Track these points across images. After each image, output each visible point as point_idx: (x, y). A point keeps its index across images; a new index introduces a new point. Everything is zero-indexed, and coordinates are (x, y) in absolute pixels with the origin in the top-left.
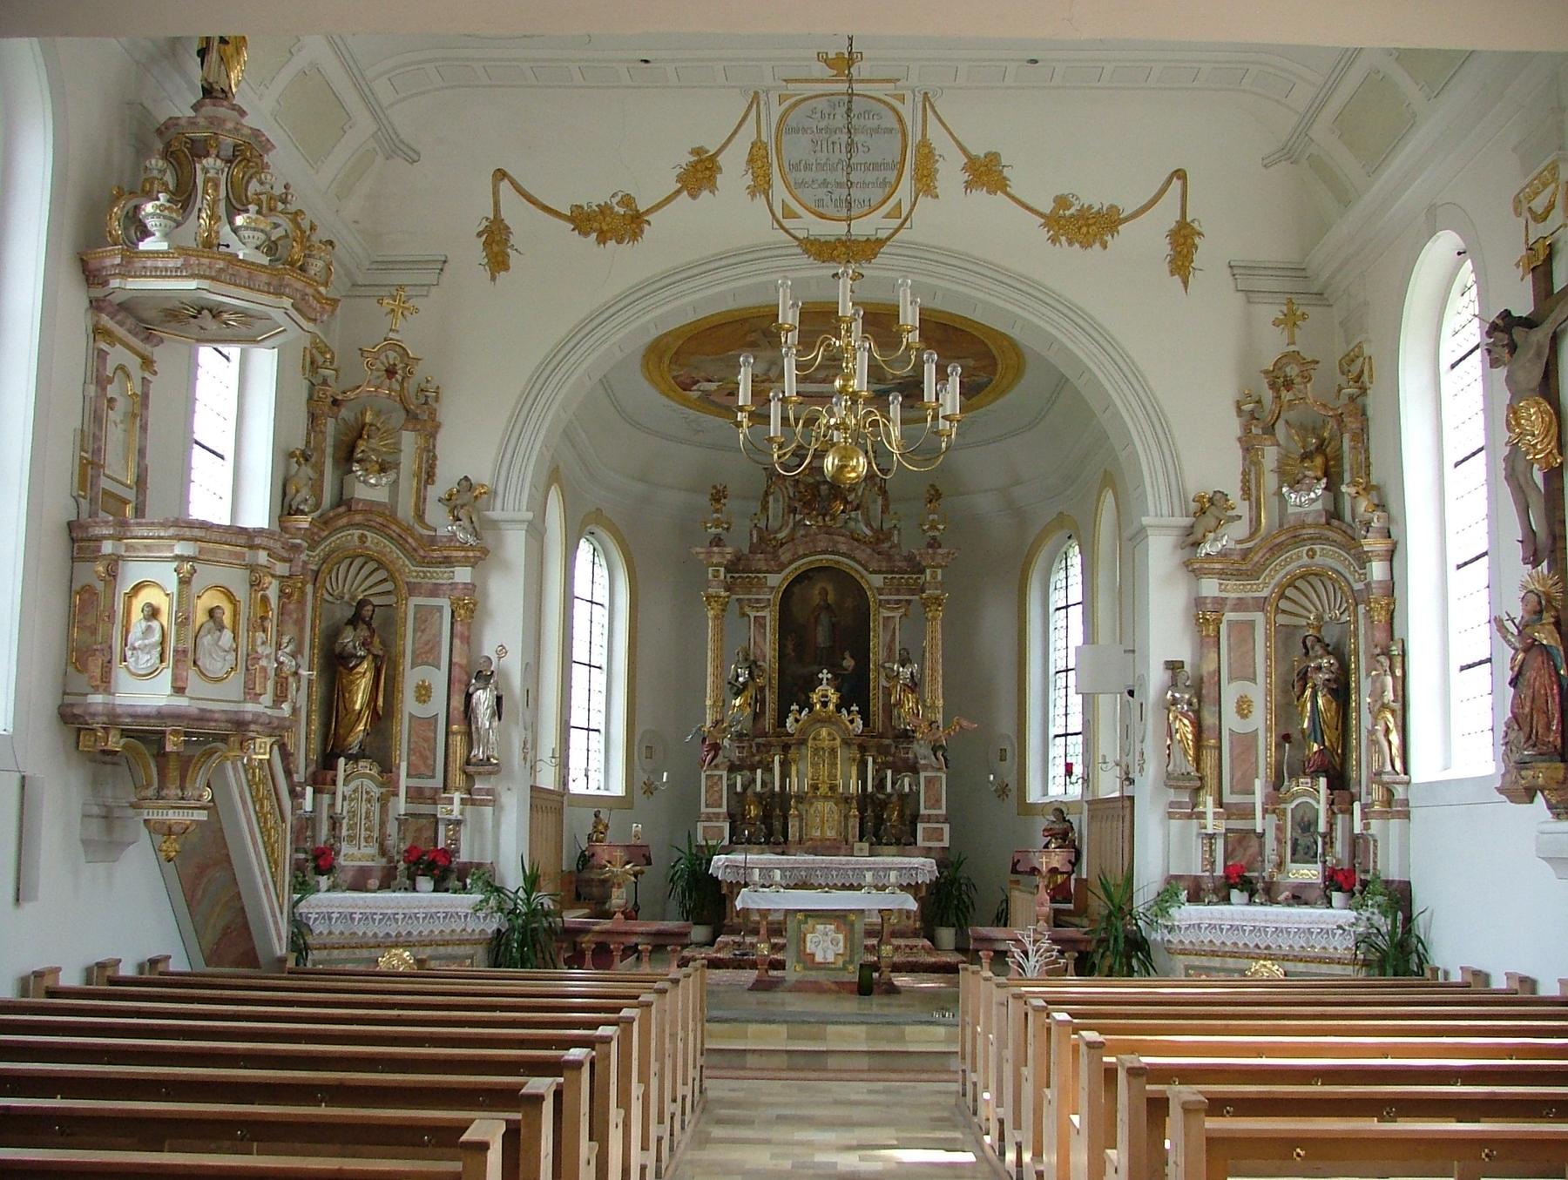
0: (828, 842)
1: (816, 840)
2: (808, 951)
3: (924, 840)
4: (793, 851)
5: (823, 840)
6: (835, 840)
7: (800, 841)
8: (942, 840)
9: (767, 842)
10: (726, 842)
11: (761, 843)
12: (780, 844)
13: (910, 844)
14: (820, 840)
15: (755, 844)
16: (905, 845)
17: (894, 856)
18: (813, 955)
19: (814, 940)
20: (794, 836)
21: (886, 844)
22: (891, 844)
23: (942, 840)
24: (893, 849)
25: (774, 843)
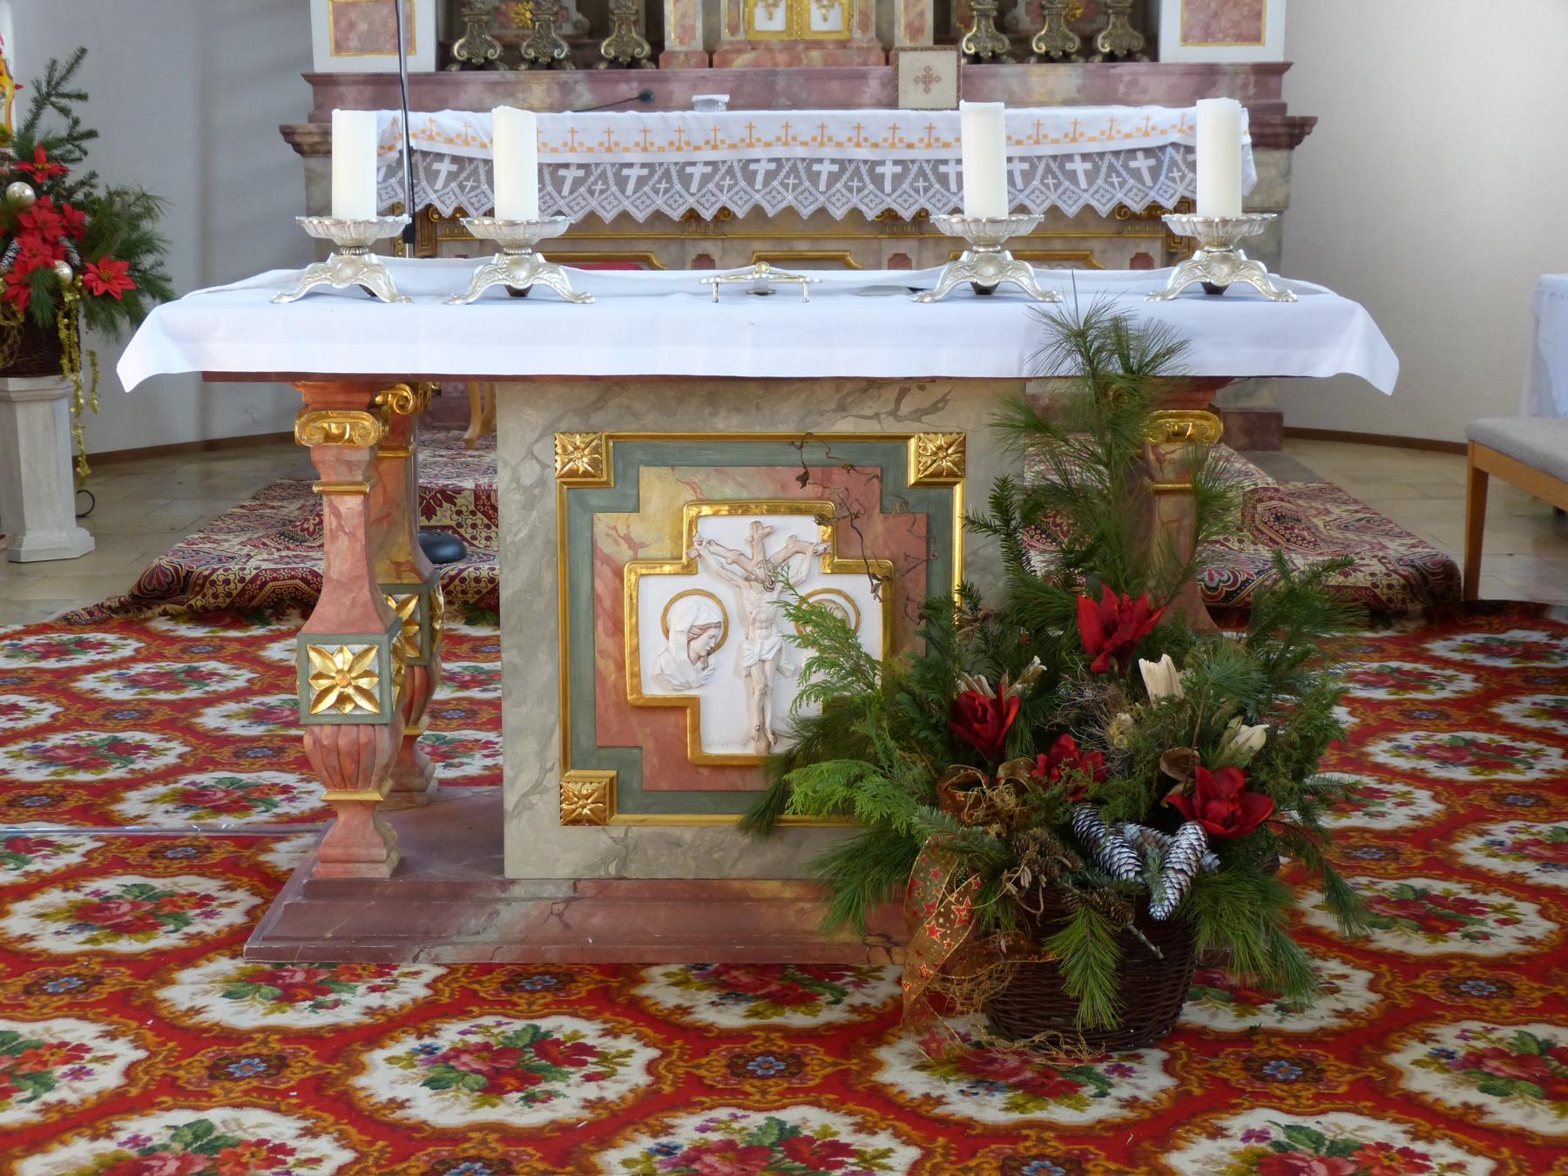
0: (816, 55)
1: (769, 49)
2: (653, 690)
3: (1185, 39)
4: (678, 90)
5: (796, 44)
6: (843, 44)
7: (711, 55)
8: (1256, 38)
9: (584, 57)
10: (424, 58)
11: (553, 64)
12: (634, 63)
13: (1130, 56)
14: (789, 46)
15: (534, 64)
16: (1111, 58)
17: (1067, 103)
18: (682, 709)
19: (687, 614)
20: (685, 32)
21: (1047, 58)
22: (1066, 58)
23: (1256, 38)
24: (1065, 77)
25: (614, 63)
